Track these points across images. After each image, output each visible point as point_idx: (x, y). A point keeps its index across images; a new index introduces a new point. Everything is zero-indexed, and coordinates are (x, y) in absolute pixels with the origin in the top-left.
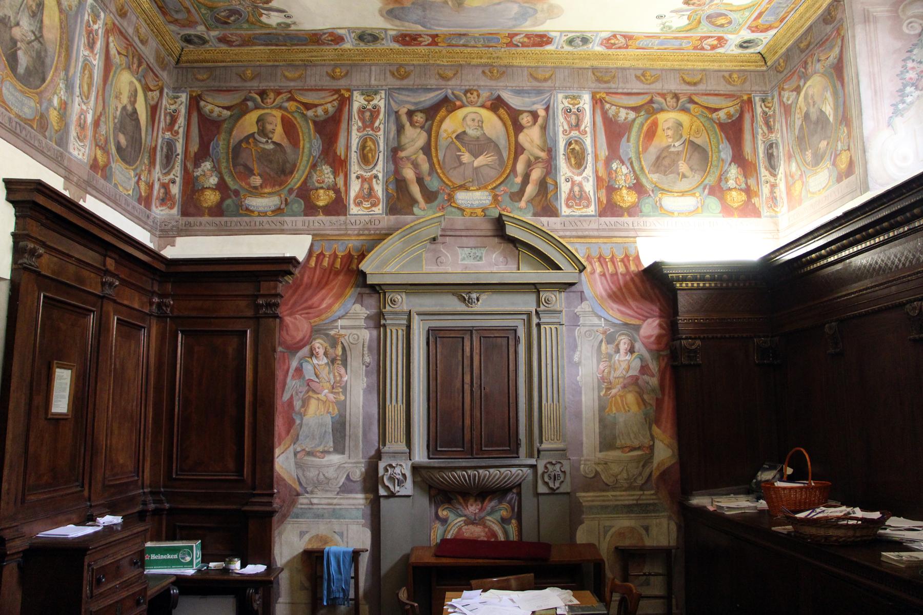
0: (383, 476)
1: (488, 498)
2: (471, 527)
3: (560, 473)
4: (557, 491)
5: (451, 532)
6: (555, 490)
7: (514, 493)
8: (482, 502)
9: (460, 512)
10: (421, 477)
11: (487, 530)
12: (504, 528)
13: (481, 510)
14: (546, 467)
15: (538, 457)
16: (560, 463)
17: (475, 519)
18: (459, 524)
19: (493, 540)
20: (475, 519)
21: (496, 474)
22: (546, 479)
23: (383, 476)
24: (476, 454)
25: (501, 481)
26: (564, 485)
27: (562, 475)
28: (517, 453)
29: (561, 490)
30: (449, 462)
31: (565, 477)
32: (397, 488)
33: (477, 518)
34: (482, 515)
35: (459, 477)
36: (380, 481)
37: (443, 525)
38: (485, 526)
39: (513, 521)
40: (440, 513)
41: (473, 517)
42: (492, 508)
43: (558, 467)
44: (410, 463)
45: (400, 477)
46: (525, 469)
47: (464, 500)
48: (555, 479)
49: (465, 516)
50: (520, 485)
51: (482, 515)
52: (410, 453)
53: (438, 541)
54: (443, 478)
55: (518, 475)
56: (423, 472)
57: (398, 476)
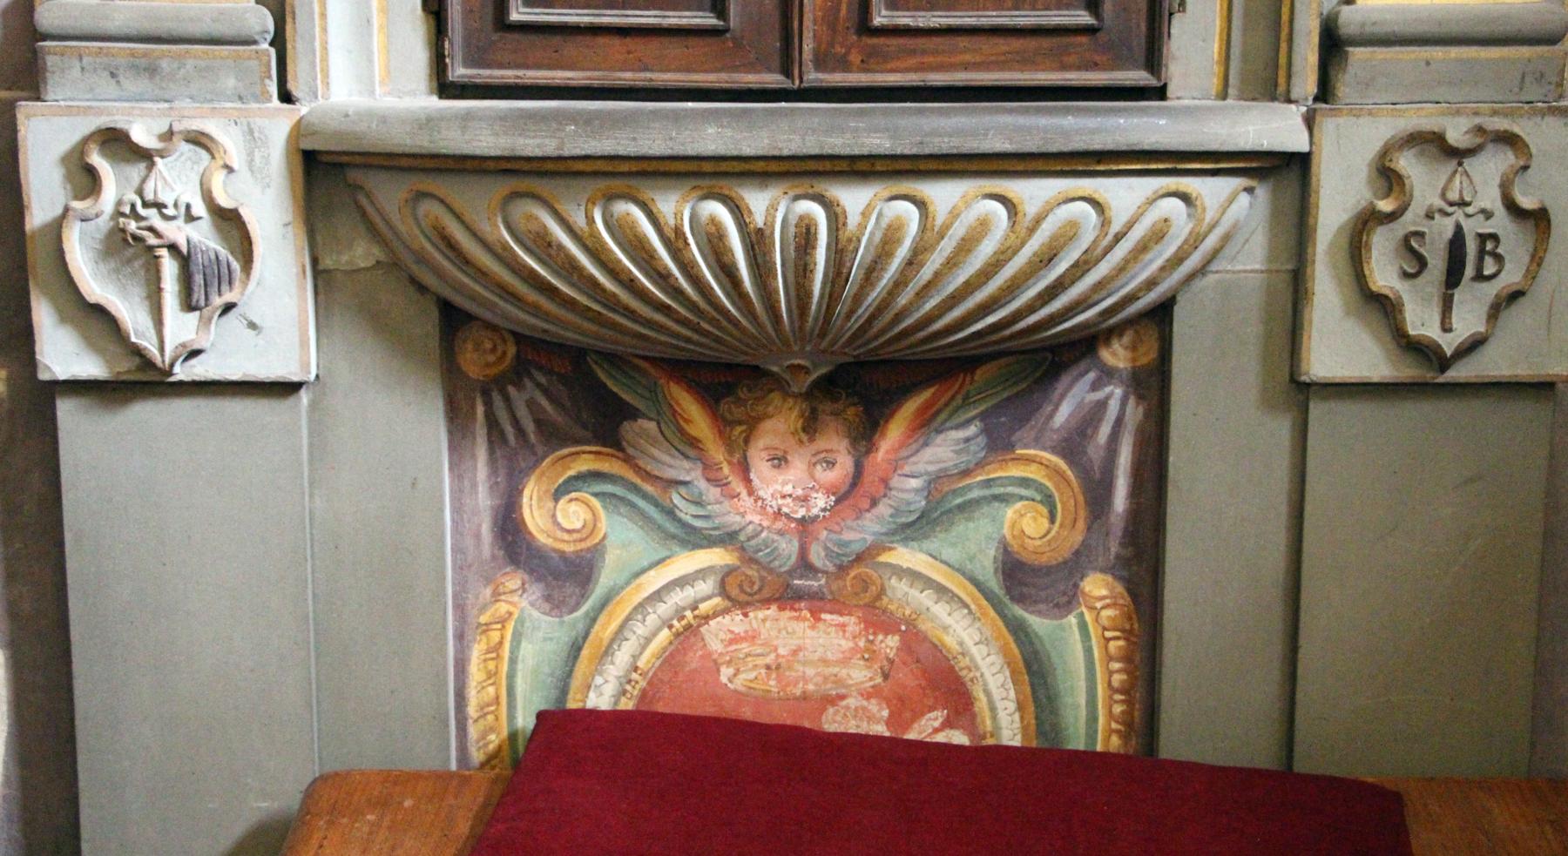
0: (56, 229)
1: (910, 407)
2: (768, 622)
3: (1501, 223)
4: (1458, 373)
5: (622, 657)
6: (1444, 362)
7: (1108, 374)
8: (865, 433)
9: (686, 511)
10: (374, 233)
11: (893, 641)
12: (1018, 630)
13: (849, 495)
14: (1387, 177)
15: (1325, 93)
16: (1509, 140)
17: (805, 566)
18: (679, 597)
19: (929, 728)
20: (805, 566)
21: (983, 227)
22: (1384, 275)
23: (56, 229)
24: (821, 63)
25: (1013, 288)
26: (1520, 318)
27: (1514, 242)
28: (1153, 59)
29: (1491, 364)
30: (587, 119)
31: (1537, 259)
32: (180, 327)
33: (817, 556)
34: (863, 530)
35: (675, 242)
36: (38, 257)
37: (556, 604)
38: (878, 619)
39: (1097, 586)
40: (535, 513)
41: (788, 548)
42: (937, 483)
43: (1489, 169)
44: (278, 125)
45: (202, 236)
46: (1212, 190)
47: (723, 424)
48: (1453, 276)
49: (728, 538)
50: (1163, 312)
51: (863, 530)
52: (279, 41)
53: (525, 721)
54: (542, 245)
55: (1158, 234)
56: (389, 195)
57: (177, 232)
